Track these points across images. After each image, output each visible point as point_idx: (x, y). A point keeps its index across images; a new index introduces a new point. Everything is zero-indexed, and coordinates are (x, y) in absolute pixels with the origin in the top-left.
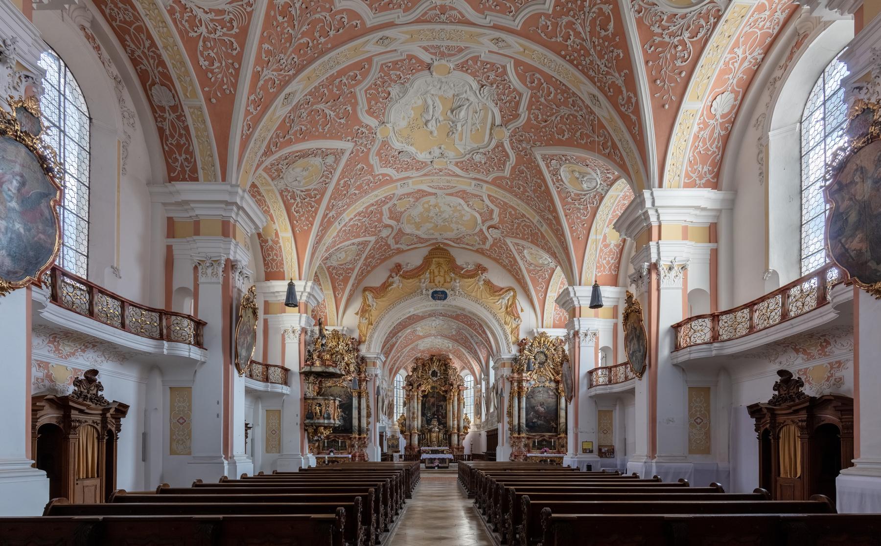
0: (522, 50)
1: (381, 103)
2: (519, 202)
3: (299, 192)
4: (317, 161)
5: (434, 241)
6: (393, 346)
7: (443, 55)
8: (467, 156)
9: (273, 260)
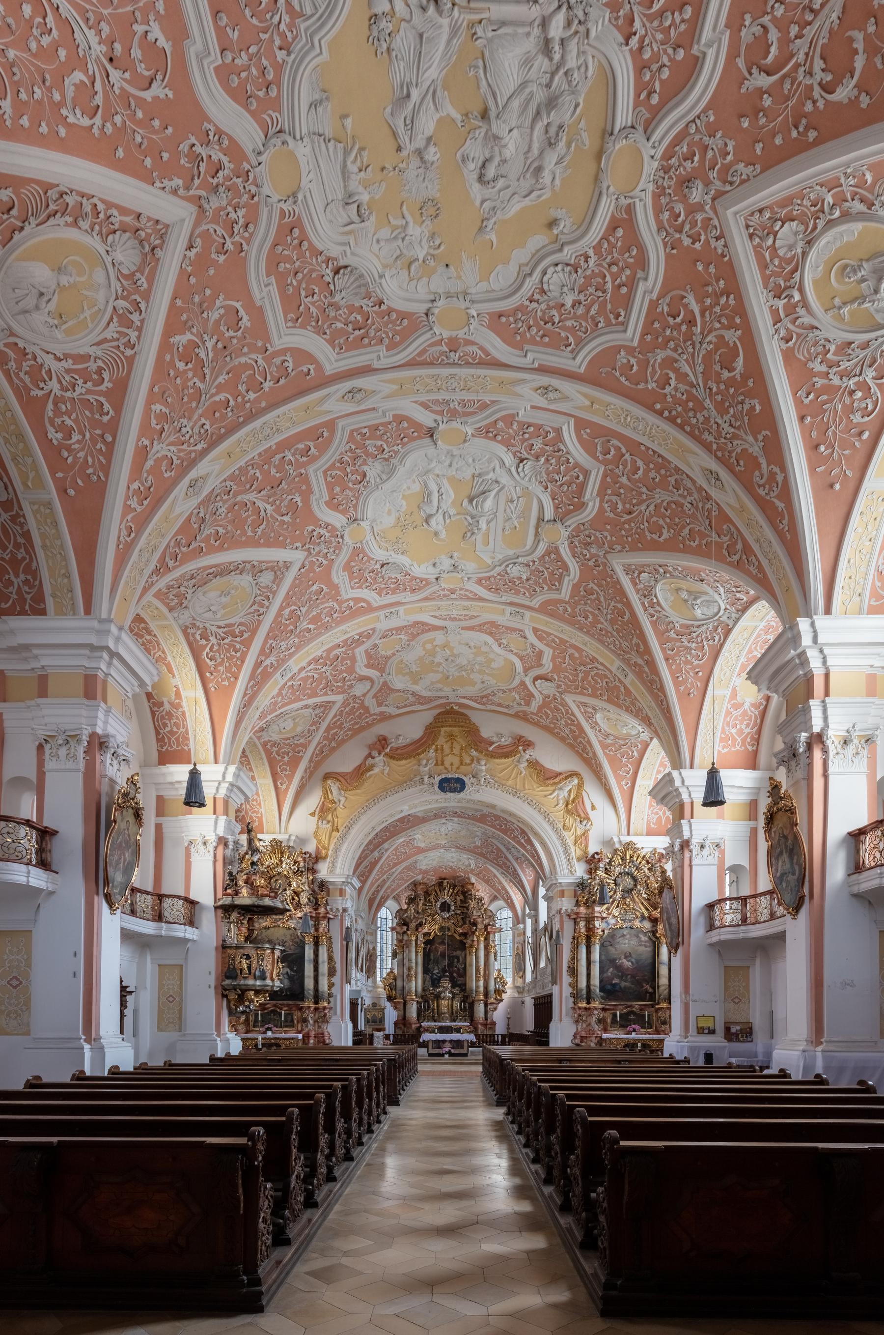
0: (588, 403)
1: (351, 489)
2: (587, 638)
3: (214, 629)
4: (245, 580)
5: (443, 701)
6: (374, 864)
7: (453, 414)
8: (498, 569)
9: (172, 733)
